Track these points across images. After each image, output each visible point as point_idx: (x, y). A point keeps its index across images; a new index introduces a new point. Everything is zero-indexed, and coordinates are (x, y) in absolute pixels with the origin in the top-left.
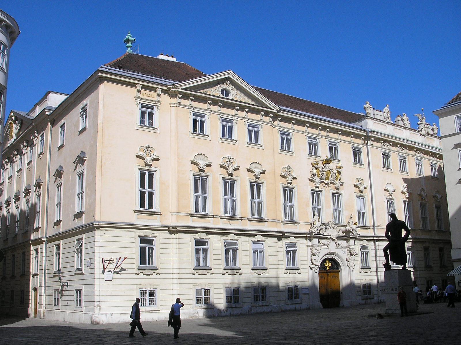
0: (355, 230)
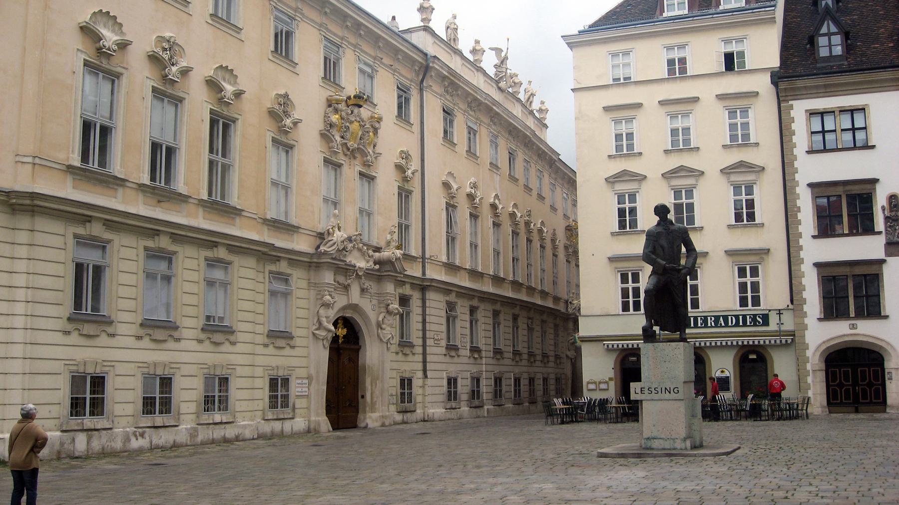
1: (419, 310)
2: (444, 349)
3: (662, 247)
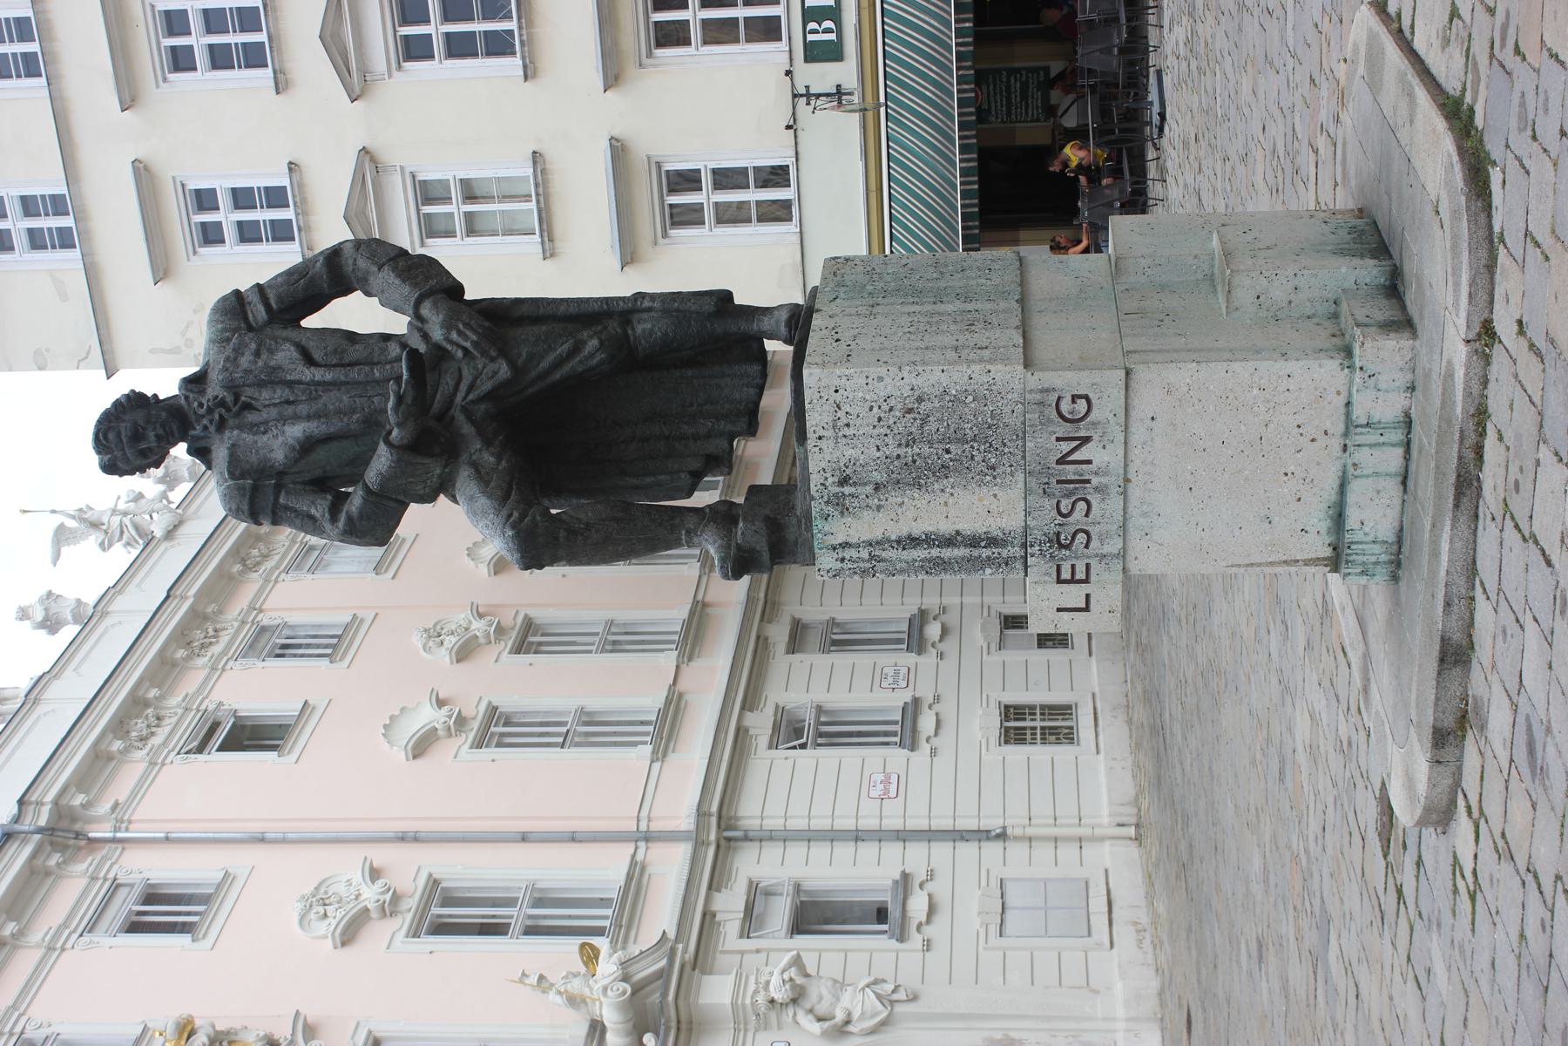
0: (624, 964)
1: (797, 851)
2: (922, 660)
3: (307, 446)
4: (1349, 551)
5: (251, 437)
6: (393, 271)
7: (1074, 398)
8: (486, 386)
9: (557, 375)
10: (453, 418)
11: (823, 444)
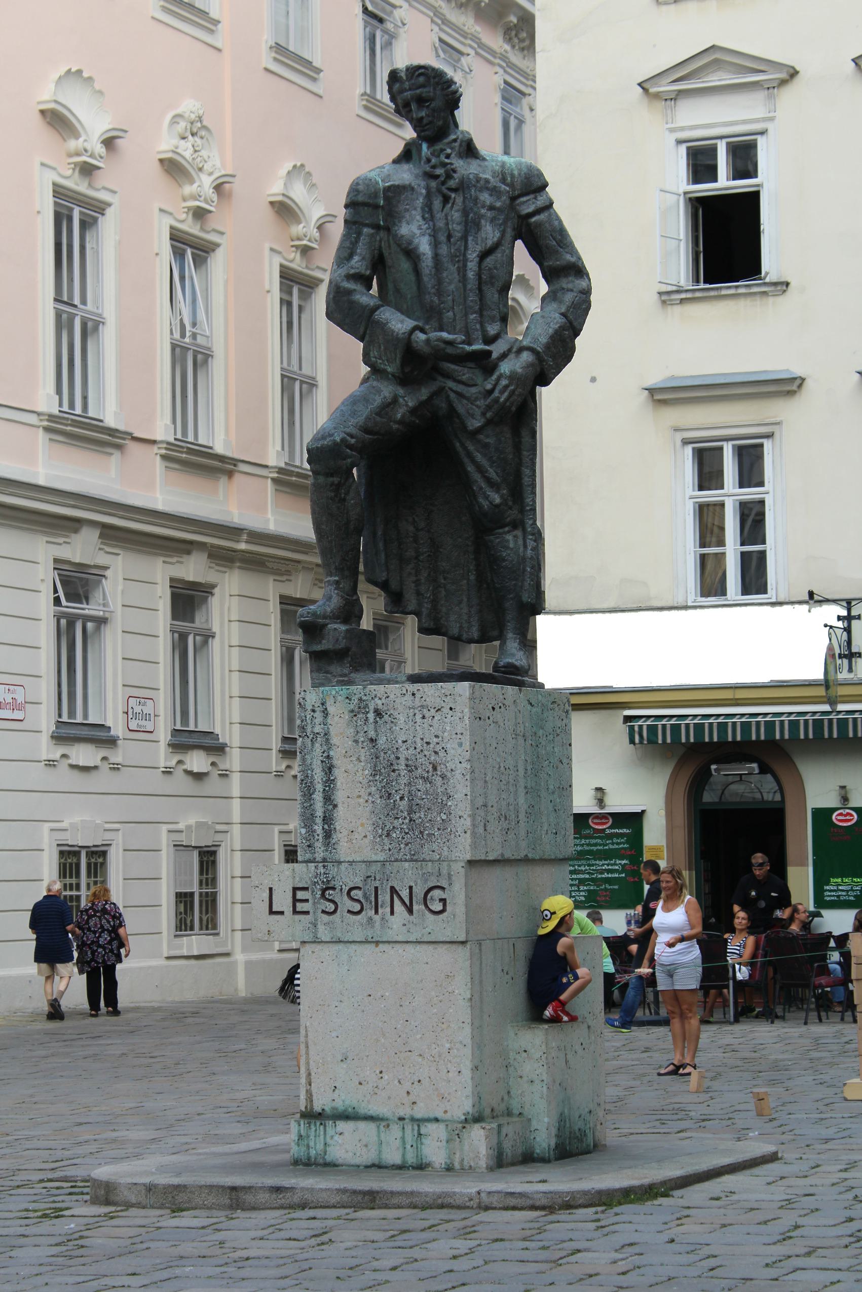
3: (411, 254)
4: (318, 1124)
5: (420, 205)
6: (560, 327)
7: (443, 901)
8: (461, 409)
9: (470, 468)
10: (435, 380)
11: (409, 697)
